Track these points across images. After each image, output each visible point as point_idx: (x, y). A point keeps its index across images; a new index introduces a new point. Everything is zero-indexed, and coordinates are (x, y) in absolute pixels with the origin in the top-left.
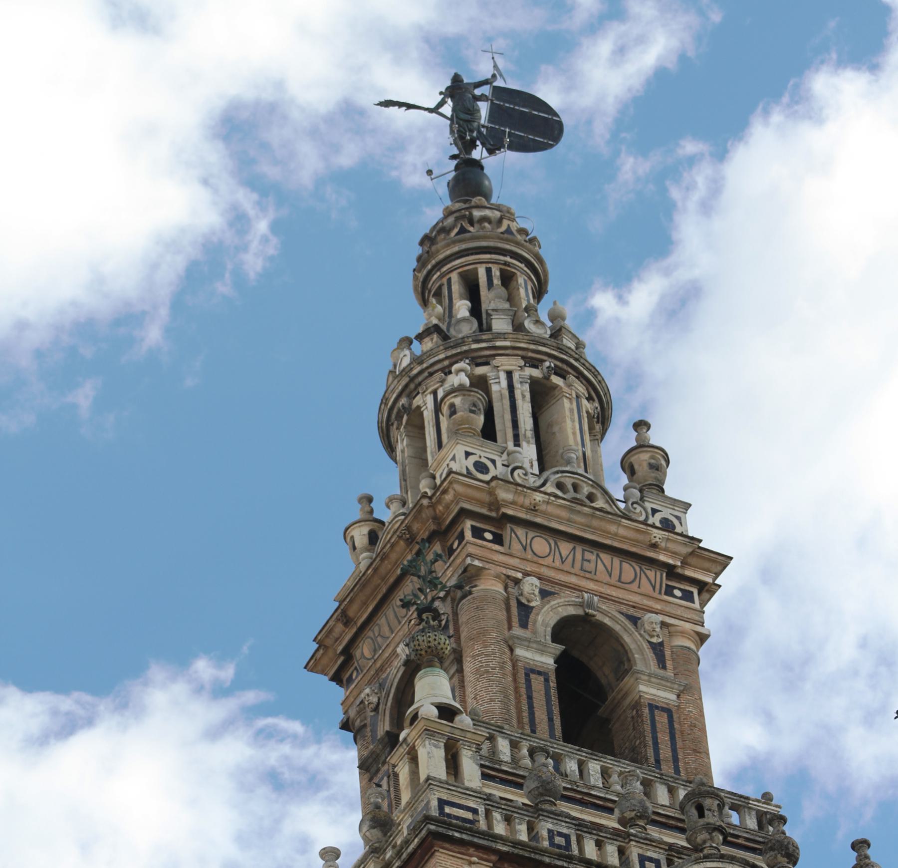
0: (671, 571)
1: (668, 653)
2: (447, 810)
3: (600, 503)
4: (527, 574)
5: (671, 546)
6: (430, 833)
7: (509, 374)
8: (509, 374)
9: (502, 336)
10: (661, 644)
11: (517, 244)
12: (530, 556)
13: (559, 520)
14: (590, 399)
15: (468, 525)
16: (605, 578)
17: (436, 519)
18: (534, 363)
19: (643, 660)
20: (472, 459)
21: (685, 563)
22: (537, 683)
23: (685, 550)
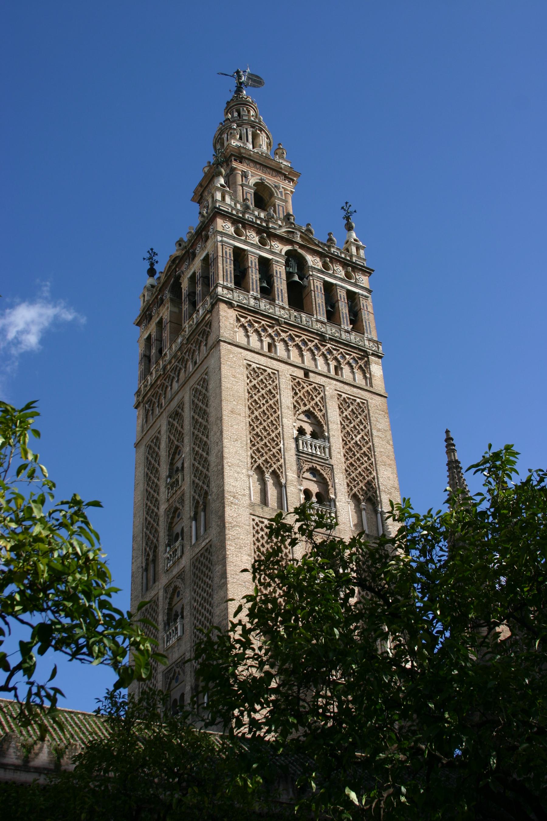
7: (247, 129)
8: (247, 129)
15: (233, 158)
17: (225, 157)
19: (277, 194)
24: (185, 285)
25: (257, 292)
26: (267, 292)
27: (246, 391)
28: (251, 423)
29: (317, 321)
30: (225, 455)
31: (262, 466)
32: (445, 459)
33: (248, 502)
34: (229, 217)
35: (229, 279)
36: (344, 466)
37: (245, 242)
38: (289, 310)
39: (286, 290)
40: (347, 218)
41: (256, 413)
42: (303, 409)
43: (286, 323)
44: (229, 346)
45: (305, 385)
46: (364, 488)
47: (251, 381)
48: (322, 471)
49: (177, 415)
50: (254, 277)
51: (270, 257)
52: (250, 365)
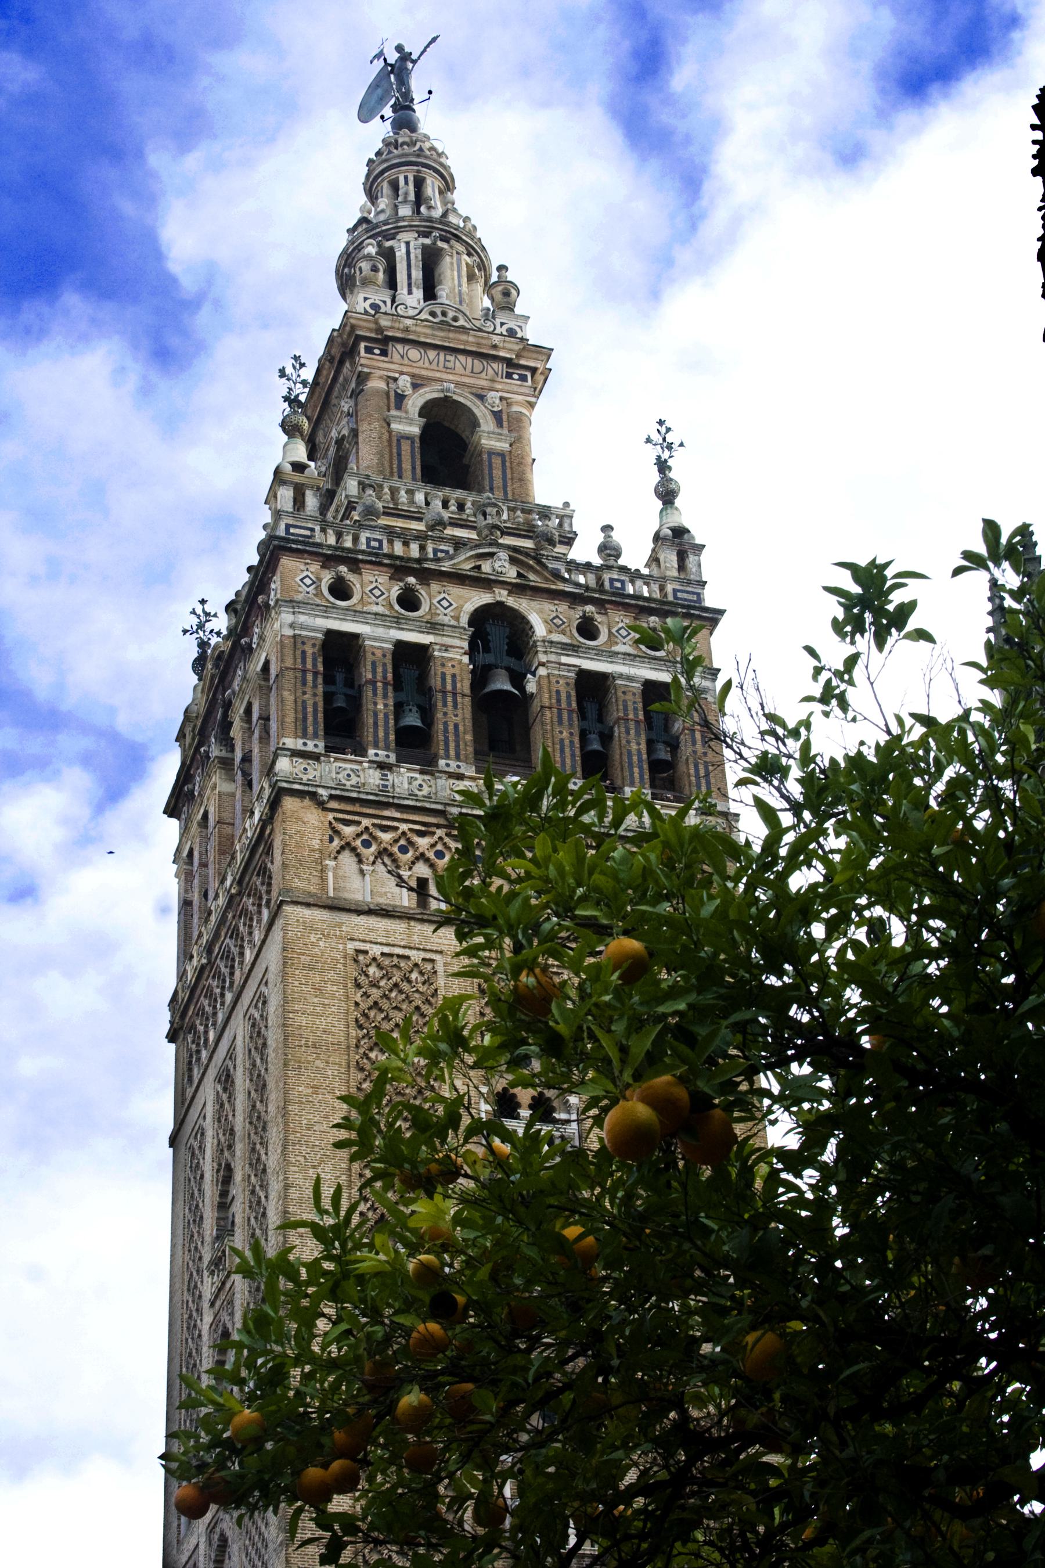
0: (509, 362)
1: (505, 417)
2: (292, 530)
3: (461, 322)
4: (402, 373)
5: (507, 345)
6: (275, 546)
7: (408, 243)
8: (408, 243)
9: (403, 219)
10: (501, 411)
11: (426, 157)
12: (406, 361)
13: (426, 335)
14: (469, 254)
15: (363, 345)
16: (462, 371)
18: (426, 235)
19: (487, 424)
20: (369, 302)
21: (518, 356)
22: (406, 447)
23: (517, 347)
24: (236, 732)
25: (387, 748)
27: (353, 1024)
34: (310, 553)
35: (310, 729)
37: (357, 614)
39: (469, 724)
40: (663, 466)
44: (307, 912)
47: (366, 995)
49: (226, 1079)
50: (380, 706)
51: (425, 639)
52: (366, 952)
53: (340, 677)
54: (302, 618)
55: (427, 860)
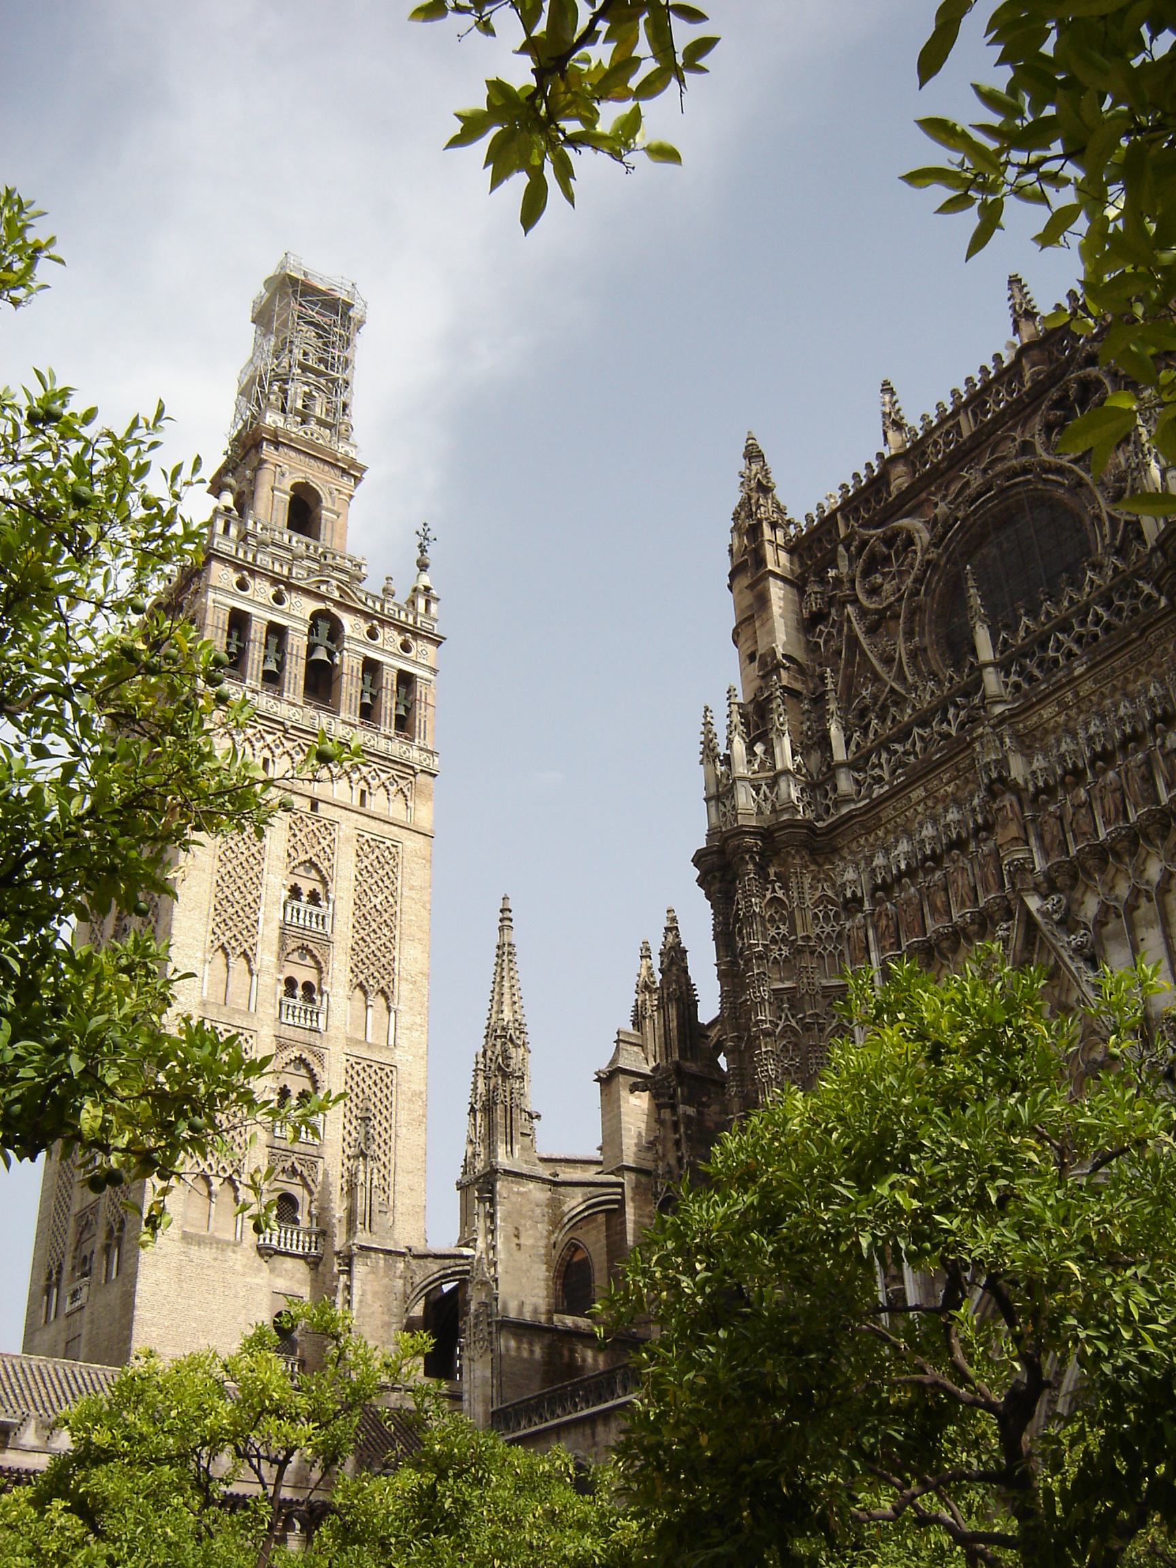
0: (343, 471)
17: (254, 440)
19: (326, 502)
26: (272, 679)
28: (220, 882)
29: (344, 722)
30: (173, 931)
31: (226, 945)
32: (496, 940)
33: (198, 1000)
36: (351, 942)
38: (301, 707)
41: (229, 867)
42: (303, 857)
43: (293, 727)
45: (309, 823)
46: (376, 974)
48: (315, 952)
53: (235, 634)
54: (220, 598)
55: (270, 748)
